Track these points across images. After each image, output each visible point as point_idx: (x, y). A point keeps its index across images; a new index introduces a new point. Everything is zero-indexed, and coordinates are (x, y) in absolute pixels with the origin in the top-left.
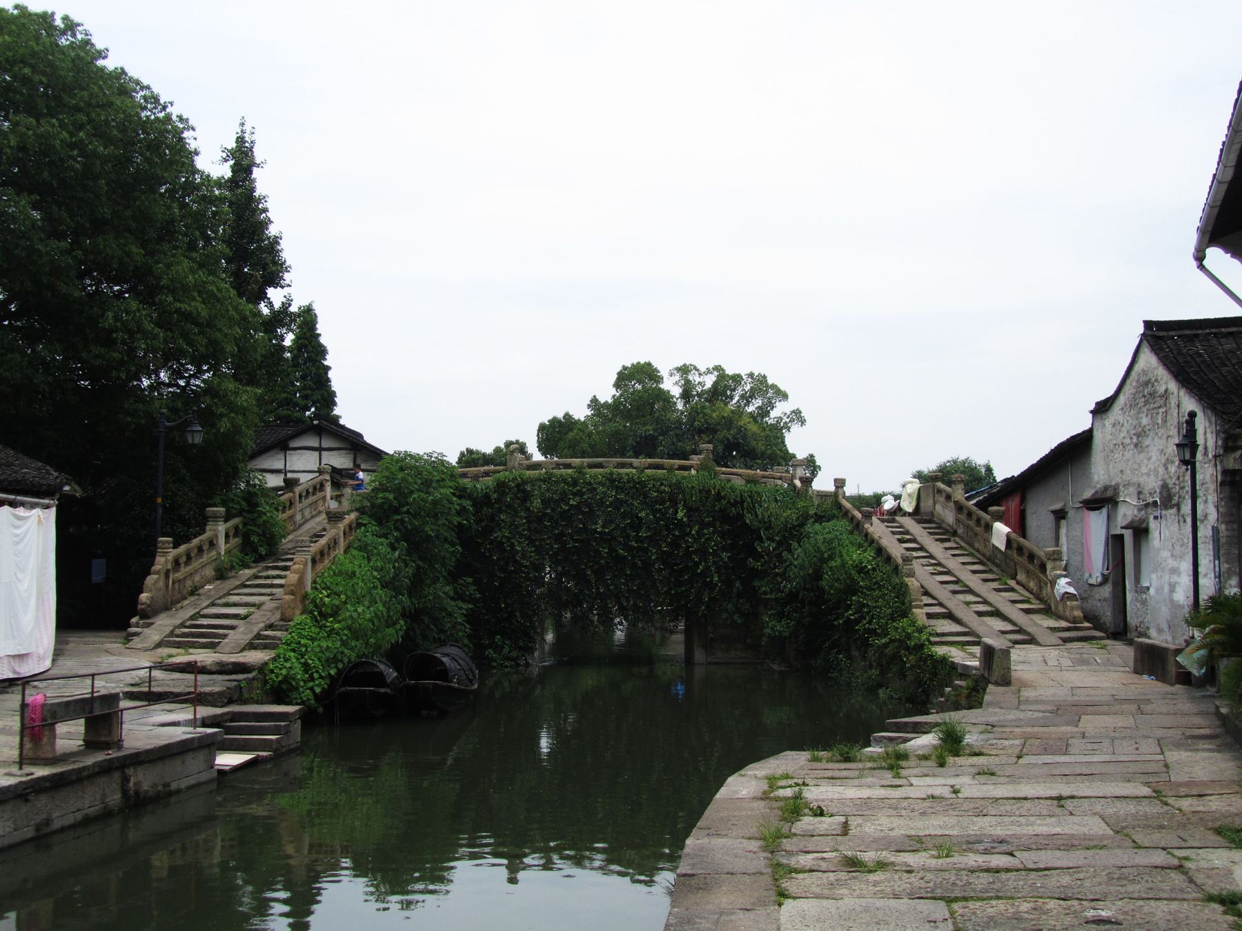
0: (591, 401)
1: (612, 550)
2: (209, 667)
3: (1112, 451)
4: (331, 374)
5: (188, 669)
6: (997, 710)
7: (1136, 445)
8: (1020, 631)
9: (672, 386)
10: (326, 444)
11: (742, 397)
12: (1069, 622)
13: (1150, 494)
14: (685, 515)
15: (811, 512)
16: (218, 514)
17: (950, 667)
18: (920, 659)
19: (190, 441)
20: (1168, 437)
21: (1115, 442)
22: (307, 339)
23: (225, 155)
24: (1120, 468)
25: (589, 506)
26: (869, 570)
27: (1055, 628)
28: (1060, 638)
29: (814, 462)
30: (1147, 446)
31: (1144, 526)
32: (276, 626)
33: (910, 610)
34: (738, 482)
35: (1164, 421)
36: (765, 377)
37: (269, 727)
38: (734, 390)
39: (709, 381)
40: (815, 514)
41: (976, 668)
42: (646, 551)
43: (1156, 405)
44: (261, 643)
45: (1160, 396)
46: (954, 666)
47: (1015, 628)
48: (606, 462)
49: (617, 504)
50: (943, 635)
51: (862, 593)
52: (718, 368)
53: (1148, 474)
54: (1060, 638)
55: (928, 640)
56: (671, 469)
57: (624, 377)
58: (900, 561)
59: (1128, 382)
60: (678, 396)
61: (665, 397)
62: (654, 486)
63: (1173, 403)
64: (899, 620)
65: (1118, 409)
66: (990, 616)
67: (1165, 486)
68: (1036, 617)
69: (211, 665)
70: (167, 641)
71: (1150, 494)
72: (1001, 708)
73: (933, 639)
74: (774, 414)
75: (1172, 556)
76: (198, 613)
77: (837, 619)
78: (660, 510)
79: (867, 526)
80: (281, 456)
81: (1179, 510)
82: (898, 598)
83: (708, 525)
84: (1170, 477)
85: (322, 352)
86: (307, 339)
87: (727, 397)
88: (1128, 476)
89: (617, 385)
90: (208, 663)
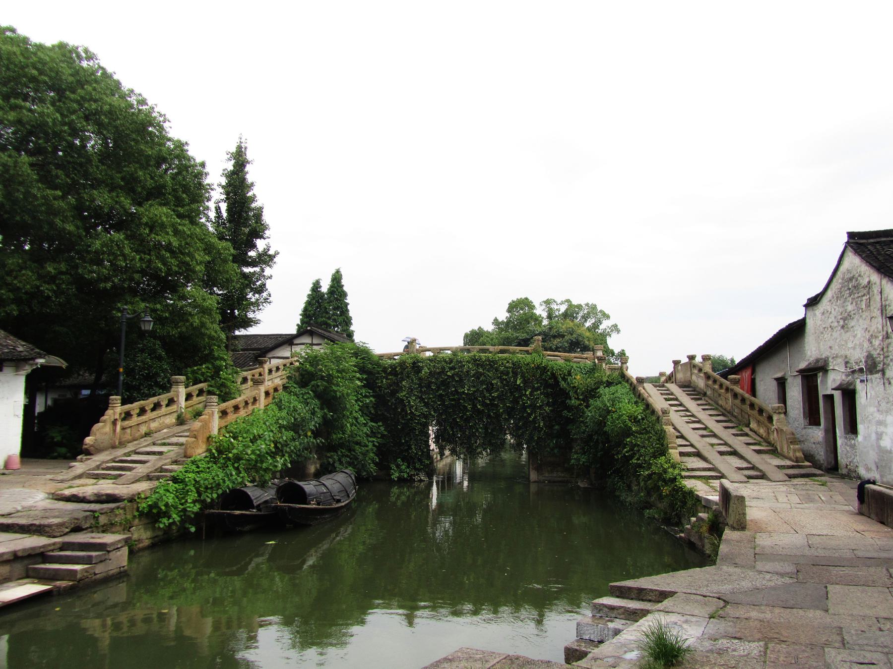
0: (494, 320)
1: (474, 406)
2: (88, 498)
3: (822, 333)
4: (349, 307)
5: (73, 499)
6: (732, 569)
7: (843, 327)
8: (753, 468)
9: (540, 311)
10: (315, 342)
11: (583, 317)
12: (793, 461)
13: (856, 363)
14: (522, 382)
15: (605, 379)
16: (179, 381)
17: (696, 499)
18: (674, 489)
19: (143, 328)
20: (871, 318)
21: (824, 326)
22: (335, 288)
23: (229, 156)
24: (829, 344)
25: (460, 376)
26: (640, 419)
27: (782, 466)
28: (787, 475)
29: (624, 354)
30: (853, 327)
31: (851, 387)
32: (179, 461)
33: (668, 451)
34: (561, 362)
35: (868, 305)
36: (595, 306)
37: (83, 557)
38: (578, 313)
39: (563, 308)
40: (607, 381)
41: (716, 504)
42: (497, 406)
43: (860, 294)
44: (155, 476)
45: (863, 287)
46: (698, 499)
47: (749, 466)
48: (472, 348)
49: (478, 376)
50: (693, 470)
51: (634, 436)
52: (568, 301)
53: (854, 348)
54: (787, 475)
55: (680, 475)
56: (514, 353)
57: (512, 307)
58: (660, 413)
59: (835, 280)
60: (545, 317)
61: (537, 320)
62: (502, 364)
63: (875, 292)
64: (659, 458)
65: (826, 301)
66: (730, 455)
67: (869, 356)
68: (766, 457)
69: (90, 496)
70: (88, 474)
71: (856, 363)
72: (736, 565)
73: (684, 473)
74: (601, 327)
75: (878, 411)
76: (135, 450)
77: (618, 453)
78: (506, 379)
79: (640, 388)
80: (290, 347)
81: (884, 374)
82: (659, 441)
83: (538, 389)
84: (875, 349)
85: (344, 295)
86: (335, 288)
87: (574, 318)
88: (836, 350)
89: (509, 311)
90: (88, 494)
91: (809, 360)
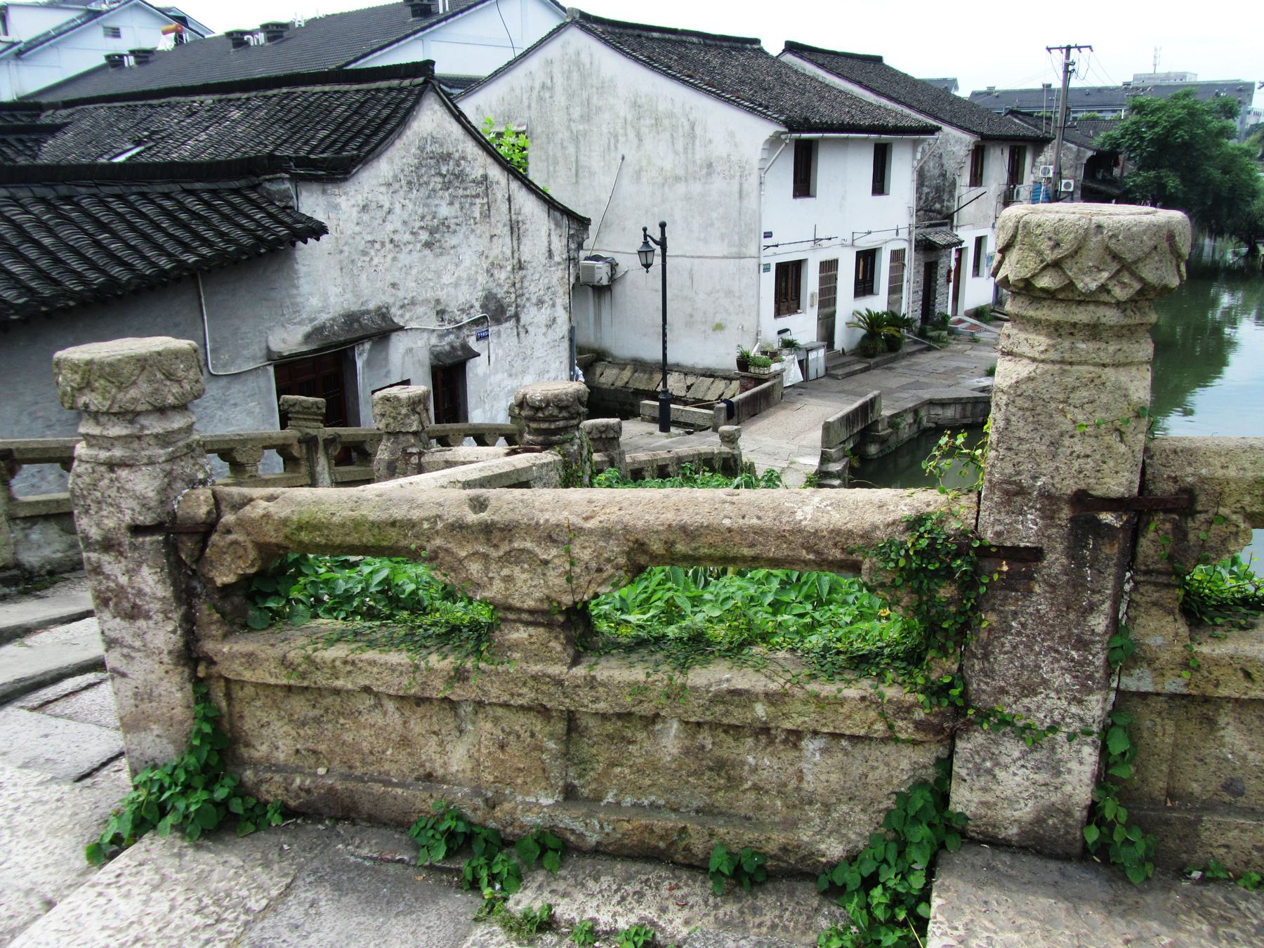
3: (364, 253)
7: (428, 245)
13: (463, 311)
20: (492, 237)
30: (454, 247)
35: (486, 215)
43: (468, 192)
45: (474, 181)
53: (456, 285)
63: (499, 196)
67: (489, 297)
71: (463, 311)
81: (518, 320)
84: (499, 285)
88: (410, 288)
91: (312, 320)
